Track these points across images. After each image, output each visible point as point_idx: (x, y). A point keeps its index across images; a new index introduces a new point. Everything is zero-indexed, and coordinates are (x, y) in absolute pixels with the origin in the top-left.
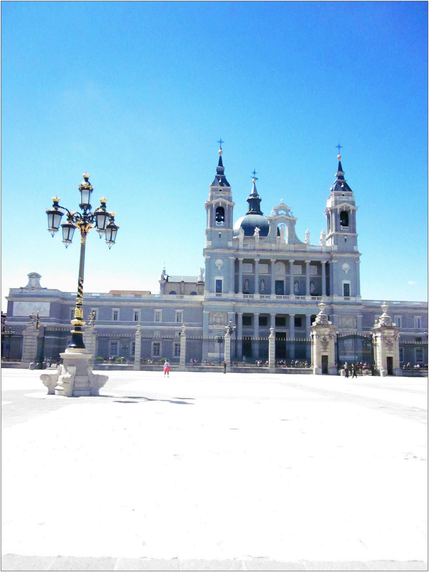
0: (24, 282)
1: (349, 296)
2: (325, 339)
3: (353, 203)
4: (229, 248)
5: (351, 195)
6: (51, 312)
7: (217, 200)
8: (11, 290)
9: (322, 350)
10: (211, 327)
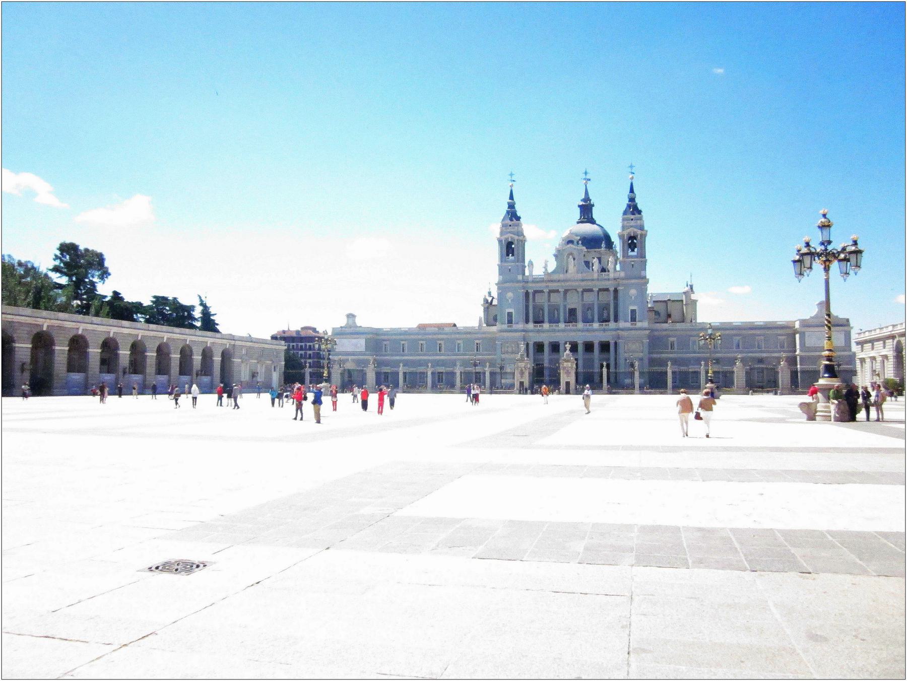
0: (342, 322)
2: (522, 370)
3: (642, 228)
4: (518, 282)
5: (641, 219)
6: (366, 346)
7: (506, 236)
8: (333, 329)
10: (503, 356)
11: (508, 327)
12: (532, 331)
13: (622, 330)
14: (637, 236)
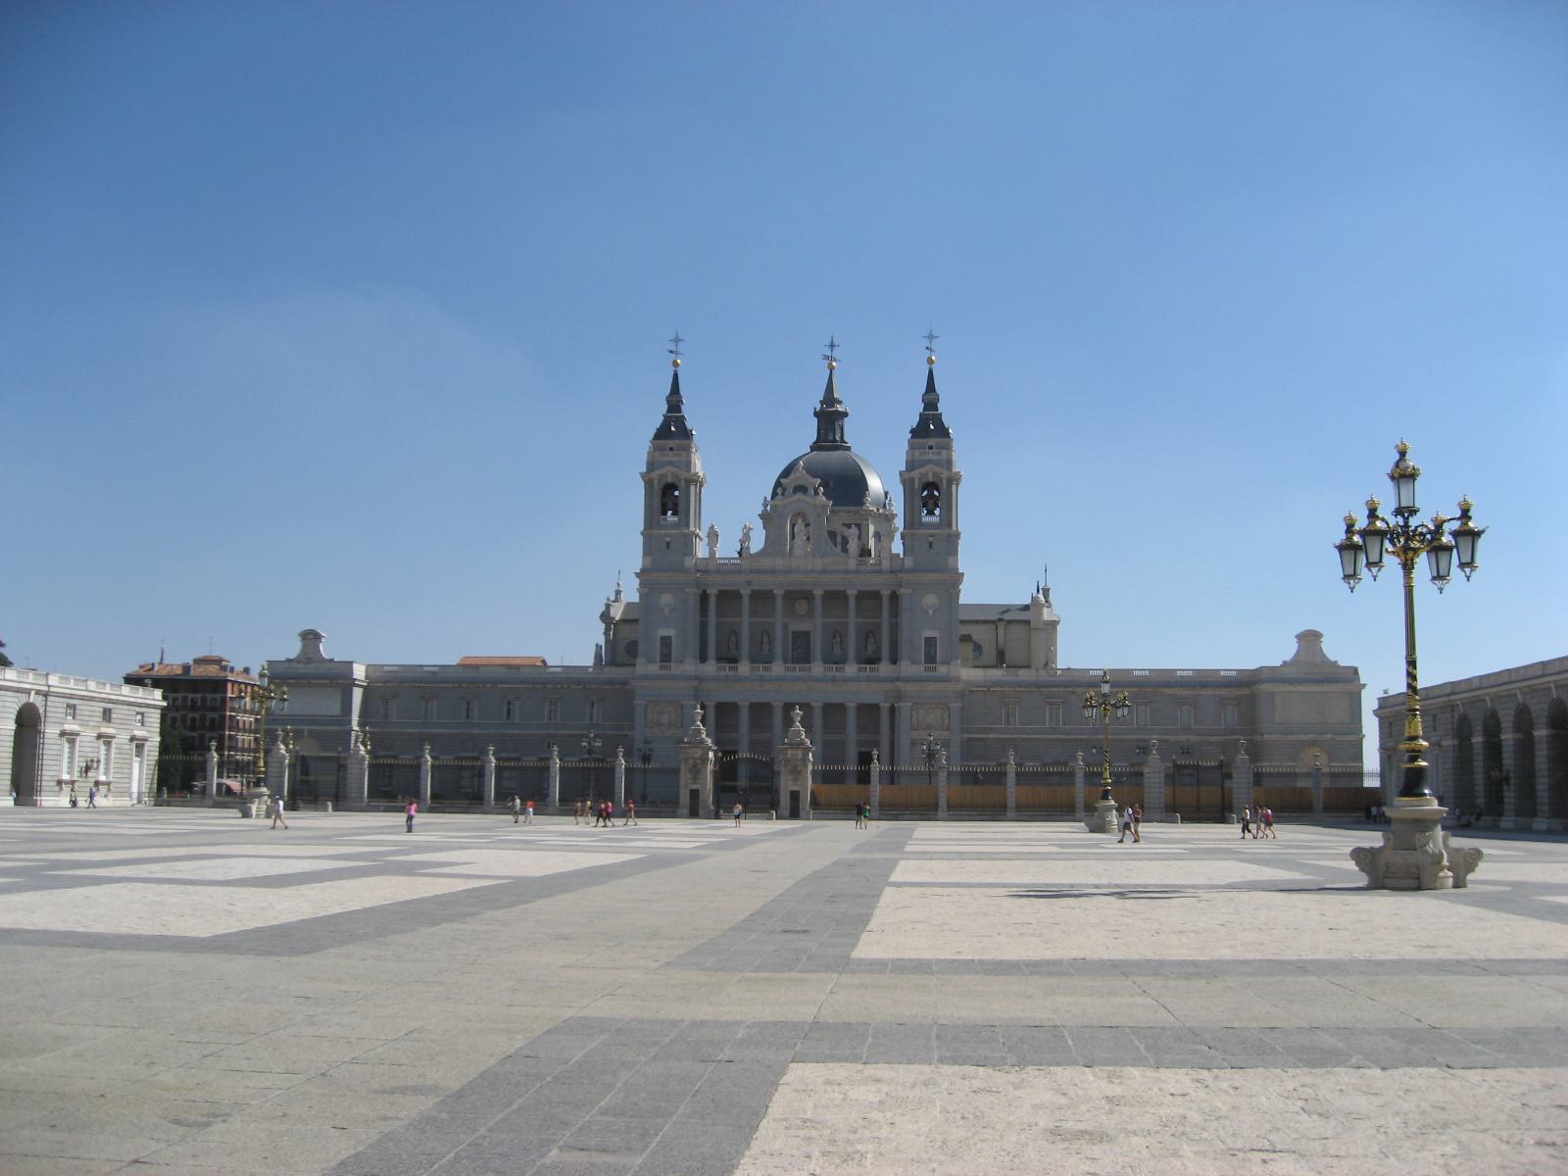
0: (292, 649)
1: (935, 663)
2: (695, 765)
3: (949, 463)
7: (660, 472)
9: (690, 781)
11: (661, 667)
12: (714, 679)
13: (908, 680)
14: (941, 480)
